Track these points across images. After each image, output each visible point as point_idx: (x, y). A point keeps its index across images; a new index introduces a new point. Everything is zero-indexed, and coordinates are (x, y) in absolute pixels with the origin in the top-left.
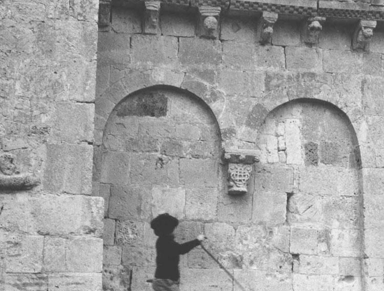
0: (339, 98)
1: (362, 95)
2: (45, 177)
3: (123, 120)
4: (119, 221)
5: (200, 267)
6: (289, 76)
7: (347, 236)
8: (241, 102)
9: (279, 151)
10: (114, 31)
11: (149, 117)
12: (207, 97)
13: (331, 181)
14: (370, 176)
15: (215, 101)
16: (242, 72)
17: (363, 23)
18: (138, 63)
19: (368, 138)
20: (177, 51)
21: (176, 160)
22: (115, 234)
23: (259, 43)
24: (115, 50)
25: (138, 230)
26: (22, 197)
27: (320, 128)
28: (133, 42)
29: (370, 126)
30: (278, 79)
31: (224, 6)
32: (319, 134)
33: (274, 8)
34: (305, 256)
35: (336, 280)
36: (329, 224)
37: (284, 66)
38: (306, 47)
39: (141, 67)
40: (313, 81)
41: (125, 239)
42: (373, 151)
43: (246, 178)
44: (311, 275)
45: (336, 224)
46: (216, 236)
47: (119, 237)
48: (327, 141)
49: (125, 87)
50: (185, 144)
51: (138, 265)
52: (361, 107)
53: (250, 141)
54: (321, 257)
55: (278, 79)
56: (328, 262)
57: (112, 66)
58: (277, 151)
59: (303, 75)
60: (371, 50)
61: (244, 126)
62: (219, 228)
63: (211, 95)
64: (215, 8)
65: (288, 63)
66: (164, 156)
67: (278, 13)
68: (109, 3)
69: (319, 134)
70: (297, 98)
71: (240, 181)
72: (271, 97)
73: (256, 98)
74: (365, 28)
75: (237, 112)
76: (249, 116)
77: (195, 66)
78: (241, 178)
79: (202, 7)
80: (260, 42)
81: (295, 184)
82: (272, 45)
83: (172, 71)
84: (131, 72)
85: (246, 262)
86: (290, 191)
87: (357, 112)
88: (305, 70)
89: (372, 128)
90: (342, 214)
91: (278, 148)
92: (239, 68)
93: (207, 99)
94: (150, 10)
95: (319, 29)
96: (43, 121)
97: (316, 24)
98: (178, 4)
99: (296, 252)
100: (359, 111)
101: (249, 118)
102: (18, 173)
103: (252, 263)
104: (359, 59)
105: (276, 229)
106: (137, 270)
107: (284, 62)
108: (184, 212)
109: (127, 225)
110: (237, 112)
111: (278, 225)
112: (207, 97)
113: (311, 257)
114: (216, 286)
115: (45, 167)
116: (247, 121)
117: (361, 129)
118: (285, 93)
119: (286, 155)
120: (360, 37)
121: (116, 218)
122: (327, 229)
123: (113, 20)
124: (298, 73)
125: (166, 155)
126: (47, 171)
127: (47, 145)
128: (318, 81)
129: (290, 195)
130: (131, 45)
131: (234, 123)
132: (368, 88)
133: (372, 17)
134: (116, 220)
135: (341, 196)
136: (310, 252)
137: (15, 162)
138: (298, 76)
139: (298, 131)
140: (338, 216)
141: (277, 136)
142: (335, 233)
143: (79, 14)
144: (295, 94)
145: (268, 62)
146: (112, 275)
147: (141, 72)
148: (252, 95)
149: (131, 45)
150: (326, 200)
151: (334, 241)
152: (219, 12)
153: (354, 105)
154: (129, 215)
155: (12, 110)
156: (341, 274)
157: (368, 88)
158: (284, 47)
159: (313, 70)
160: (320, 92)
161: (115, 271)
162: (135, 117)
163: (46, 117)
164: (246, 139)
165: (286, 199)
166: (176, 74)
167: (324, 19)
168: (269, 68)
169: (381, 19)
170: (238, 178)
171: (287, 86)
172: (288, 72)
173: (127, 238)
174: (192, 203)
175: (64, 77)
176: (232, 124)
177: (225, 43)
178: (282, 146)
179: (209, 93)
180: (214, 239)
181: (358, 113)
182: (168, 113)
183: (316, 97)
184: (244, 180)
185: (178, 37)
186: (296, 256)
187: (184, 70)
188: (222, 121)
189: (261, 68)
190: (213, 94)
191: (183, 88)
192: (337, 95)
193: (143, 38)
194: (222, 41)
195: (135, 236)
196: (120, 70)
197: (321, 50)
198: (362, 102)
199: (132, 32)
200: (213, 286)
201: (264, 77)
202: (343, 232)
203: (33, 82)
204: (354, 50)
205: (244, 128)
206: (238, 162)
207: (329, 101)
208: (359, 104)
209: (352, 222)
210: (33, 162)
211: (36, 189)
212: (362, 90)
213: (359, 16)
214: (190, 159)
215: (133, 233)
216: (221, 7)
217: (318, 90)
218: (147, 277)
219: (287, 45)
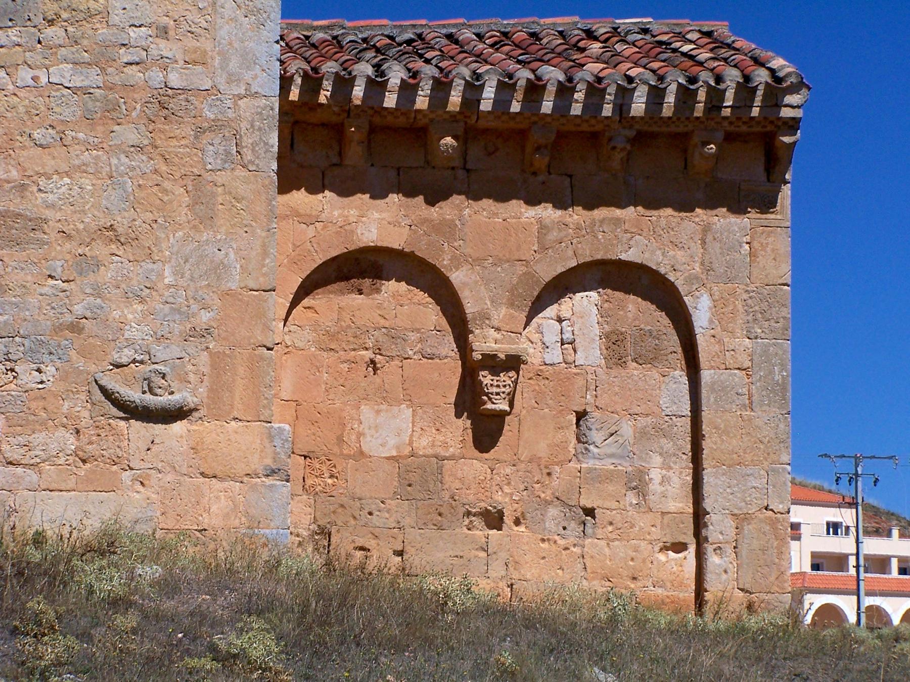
0: (661, 258)
1: (702, 250)
2: (208, 397)
4: (310, 458)
5: (435, 528)
6: (578, 223)
7: (676, 481)
9: (562, 344)
11: (353, 296)
12: (445, 263)
13: (649, 392)
14: (713, 383)
15: (457, 269)
18: (336, 213)
19: (711, 321)
21: (397, 362)
22: (304, 478)
25: (338, 472)
26: (178, 427)
30: (560, 230)
32: (630, 315)
34: (604, 511)
35: (657, 549)
36: (645, 461)
41: (320, 485)
42: (720, 342)
43: (507, 390)
44: (613, 540)
45: (657, 460)
47: (309, 482)
48: (642, 326)
50: (413, 336)
51: (340, 523)
52: (700, 271)
53: (512, 330)
54: (630, 513)
56: (643, 521)
58: (559, 344)
59: (602, 221)
62: (465, 468)
66: (378, 356)
69: (630, 315)
70: (591, 259)
71: (498, 394)
72: (548, 260)
73: (524, 262)
75: (493, 286)
76: (511, 291)
78: (498, 390)
81: (588, 397)
83: (389, 223)
84: (325, 227)
85: (508, 520)
86: (580, 409)
87: (690, 280)
89: (717, 304)
90: (667, 444)
91: (562, 339)
92: (496, 215)
93: (445, 267)
96: (204, 319)
99: (589, 506)
101: (513, 294)
102: (172, 393)
105: (557, 468)
106: (338, 531)
108: (411, 443)
109: (322, 463)
110: (493, 286)
111: (561, 464)
112: (445, 263)
113: (614, 512)
114: (461, 557)
115: (208, 384)
116: (508, 300)
117: (699, 306)
119: (575, 351)
121: (306, 453)
122: (641, 468)
125: (381, 354)
126: (211, 390)
127: (211, 354)
128: (626, 231)
129: (581, 416)
131: (489, 303)
132: (715, 239)
134: (305, 457)
135: (667, 416)
136: (614, 505)
137: (168, 377)
139: (595, 310)
140: (662, 448)
141: (560, 320)
142: (655, 475)
143: (252, 162)
146: (301, 539)
151: (655, 486)
153: (689, 268)
154: (325, 449)
155: (162, 306)
156: (665, 540)
158: (570, 176)
161: (305, 533)
163: (207, 314)
164: (508, 328)
165: (575, 422)
166: (396, 228)
170: (495, 390)
171: (574, 241)
172: (576, 217)
173: (322, 484)
174: (422, 429)
175: (232, 256)
176: (486, 304)
178: (567, 336)
180: (457, 485)
181: (695, 282)
183: (623, 257)
184: (504, 393)
186: (590, 512)
187: (409, 222)
190: (454, 258)
192: (659, 252)
194: (468, 171)
195: (336, 480)
196: (308, 226)
198: (702, 264)
200: (457, 556)
202: (671, 473)
203: (188, 266)
205: (503, 310)
207: (645, 262)
208: (697, 267)
209: (684, 457)
210: (192, 377)
211: (196, 414)
212: (704, 242)
217: (626, 246)
218: (353, 541)
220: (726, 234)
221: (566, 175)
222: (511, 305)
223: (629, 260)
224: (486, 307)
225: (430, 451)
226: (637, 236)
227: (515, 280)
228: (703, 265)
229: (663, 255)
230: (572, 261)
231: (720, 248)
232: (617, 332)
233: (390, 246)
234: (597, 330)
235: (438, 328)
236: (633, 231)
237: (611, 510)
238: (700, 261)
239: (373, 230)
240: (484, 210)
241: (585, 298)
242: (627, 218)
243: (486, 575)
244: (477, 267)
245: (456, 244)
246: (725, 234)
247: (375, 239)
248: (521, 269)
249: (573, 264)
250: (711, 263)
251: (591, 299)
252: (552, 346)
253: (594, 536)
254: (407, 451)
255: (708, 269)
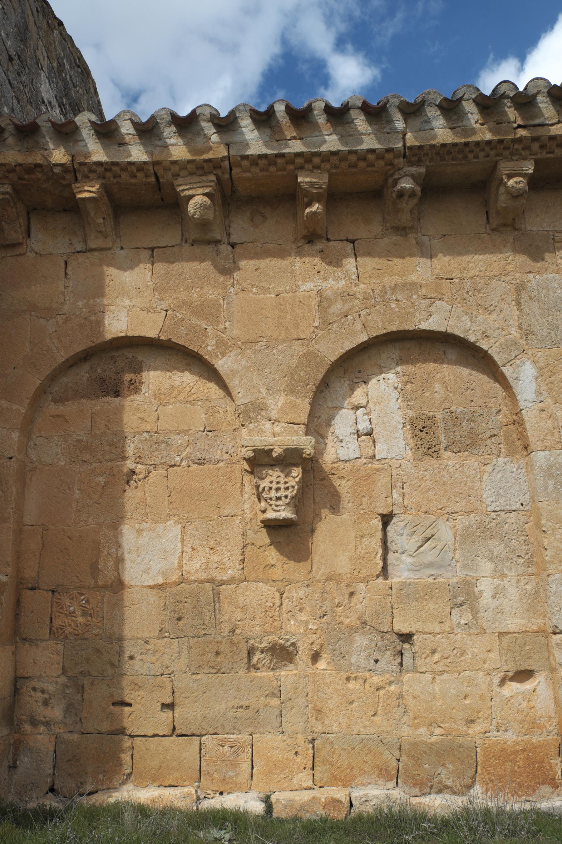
0: (469, 323)
1: (518, 313)
3: (61, 408)
4: (59, 593)
5: (214, 671)
6: (365, 293)
7: (513, 591)
8: (274, 351)
9: (359, 436)
10: (36, 253)
11: (109, 399)
12: (209, 348)
13: (469, 484)
14: (549, 467)
15: (224, 355)
16: (273, 296)
17: (505, 167)
18: (80, 304)
19: (538, 393)
20: (150, 274)
21: (161, 471)
22: (51, 618)
23: (303, 241)
24: (38, 286)
25: (92, 608)
27: (437, 387)
28: (69, 268)
29: (541, 369)
30: (345, 302)
31: (219, 172)
32: (437, 396)
33: (316, 160)
34: (425, 636)
36: (472, 569)
37: (354, 277)
38: (395, 238)
39: (84, 310)
40: (415, 297)
41: (70, 625)
43: (290, 493)
44: (442, 673)
45: (486, 567)
46: (244, 609)
47: (57, 622)
49: (57, 348)
50: (178, 440)
51: (95, 674)
52: (518, 335)
53: (295, 421)
54: (459, 637)
55: (345, 302)
57: (33, 313)
58: (356, 436)
59: (394, 288)
60: (529, 228)
61: (283, 396)
62: (248, 593)
63: (216, 345)
64: (204, 178)
65: (361, 270)
66: (139, 466)
67: (328, 171)
68: (7, 196)
70: (385, 332)
71: (278, 498)
72: (333, 336)
73: (304, 341)
74: (510, 177)
75: (268, 371)
77: (183, 295)
78: (278, 495)
79: (180, 180)
80: (305, 237)
81: (395, 496)
82: (328, 240)
83: (142, 309)
84: (67, 321)
85: (303, 656)
86: (386, 511)
87: (507, 347)
88: (396, 279)
90: (498, 548)
91: (358, 431)
92: (267, 290)
93: (209, 353)
94: (83, 199)
95: (413, 194)
97: (406, 184)
98: (133, 181)
99: (406, 631)
100: (516, 344)
101: (292, 379)
103: (315, 657)
104: (504, 246)
105: (362, 586)
106: (92, 684)
107: (354, 270)
108: (180, 566)
109: (72, 599)
110: (268, 371)
112: (209, 348)
113: (439, 636)
114: (248, 707)
116: (287, 386)
117: (522, 376)
118: (358, 326)
119: (374, 442)
120: (502, 198)
121: (53, 588)
122: (468, 578)
123: (32, 235)
124: (384, 286)
125: (142, 463)
128: (425, 297)
129: (386, 519)
130: (66, 274)
131: (264, 391)
132: (531, 298)
133: (523, 153)
134: (53, 592)
135: (494, 511)
136: (437, 628)
138: (384, 292)
139: (395, 395)
140: (491, 552)
144: (380, 324)
145: (322, 273)
146: (46, 696)
147: (86, 318)
148: (295, 336)
149: (66, 274)
150: (461, 522)
152: (212, 184)
153: (504, 333)
154: (77, 581)
156: (505, 668)
157: (531, 298)
158: (353, 242)
159: (413, 278)
160: (430, 315)
161: (51, 688)
162: (84, 401)
164: (289, 418)
165: (381, 527)
166: (150, 315)
167: (422, 170)
168: (325, 283)
169: (544, 155)
170: (273, 494)
171: (362, 313)
172: (362, 286)
173: (73, 624)
174: (193, 549)
176: (260, 392)
177: (238, 249)
179: (213, 342)
180: (239, 615)
181: (513, 348)
182: (144, 388)
183: (424, 326)
184: (286, 497)
185: (152, 249)
186: (406, 638)
187: (164, 305)
188: (239, 390)
189: (309, 285)
191: (163, 338)
192: (465, 318)
193: (88, 258)
194: (233, 246)
195: (90, 618)
196: (48, 320)
197: (426, 239)
198: (520, 327)
199: (69, 251)
200: (241, 707)
201: (314, 303)
202: (505, 582)
204: (493, 230)
205: (282, 399)
206: (272, 463)
207: (449, 330)
208: (514, 332)
209: (521, 561)
212: (519, 304)
213: (492, 153)
214: (189, 466)
215: (84, 614)
216: (217, 175)
217: (426, 314)
218: (112, 696)
219: (358, 237)
220: (544, 291)
221: (347, 240)
222: (291, 390)
223: (431, 329)
224: (261, 396)
225: (202, 576)
226: (437, 302)
227: (294, 362)
228: (521, 329)
229: (471, 320)
230: (362, 335)
231: (539, 308)
232: (423, 417)
233: (143, 334)
234: (398, 418)
235: (208, 428)
236: (433, 295)
237: (435, 635)
238: (517, 324)
239: (123, 319)
240: (253, 286)
241: (382, 381)
242: (423, 282)
243: (280, 729)
244: (248, 351)
245: (221, 327)
246: (544, 291)
247: (125, 328)
248: (299, 349)
249: (363, 338)
250: (530, 325)
251: (389, 382)
252: (347, 439)
253: (415, 670)
254: (175, 577)
255: (527, 333)
